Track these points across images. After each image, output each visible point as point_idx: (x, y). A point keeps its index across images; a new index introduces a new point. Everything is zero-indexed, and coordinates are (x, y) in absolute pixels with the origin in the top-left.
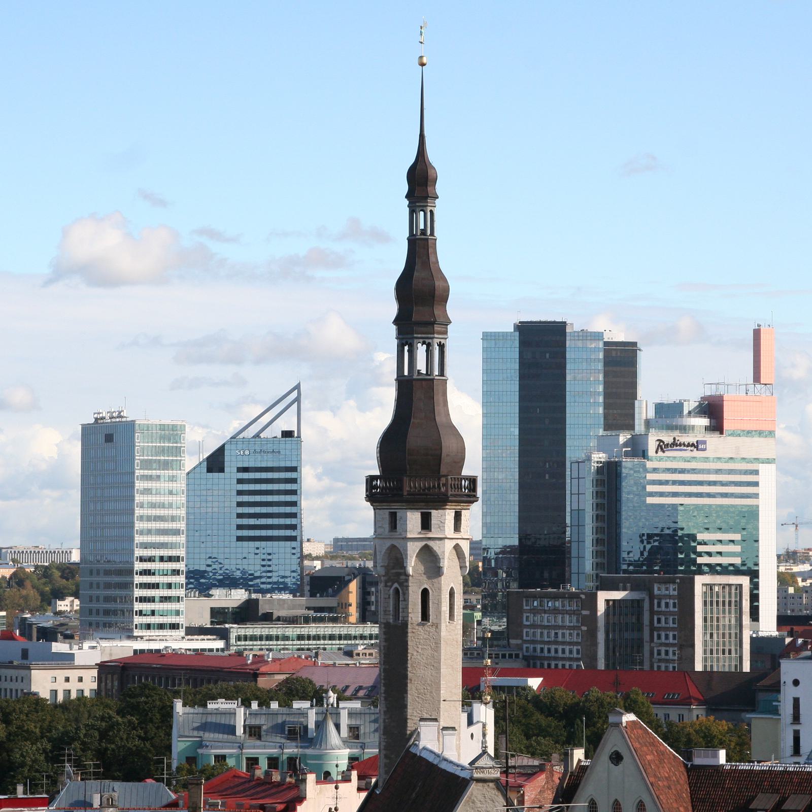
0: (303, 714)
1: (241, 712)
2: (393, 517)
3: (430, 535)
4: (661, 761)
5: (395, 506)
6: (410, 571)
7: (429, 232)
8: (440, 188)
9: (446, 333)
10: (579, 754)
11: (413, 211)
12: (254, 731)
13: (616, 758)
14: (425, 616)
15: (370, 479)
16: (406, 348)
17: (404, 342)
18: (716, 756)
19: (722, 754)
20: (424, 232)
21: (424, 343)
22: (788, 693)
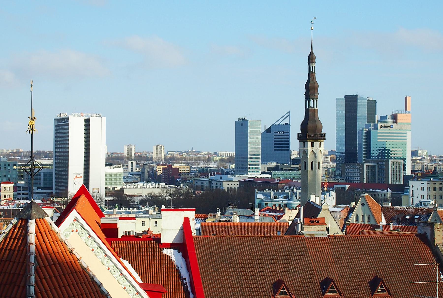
0: (288, 193)
1: (272, 192)
2: (304, 143)
3: (313, 148)
4: (374, 206)
5: (305, 141)
6: (308, 157)
7: (313, 72)
8: (316, 60)
9: (318, 97)
10: (354, 204)
11: (309, 66)
12: (275, 197)
13: (363, 205)
14: (312, 168)
15: (298, 134)
16: (308, 101)
17: (307, 99)
18: (388, 204)
19: (390, 204)
20: (312, 72)
21: (312, 100)
22: (411, 189)
